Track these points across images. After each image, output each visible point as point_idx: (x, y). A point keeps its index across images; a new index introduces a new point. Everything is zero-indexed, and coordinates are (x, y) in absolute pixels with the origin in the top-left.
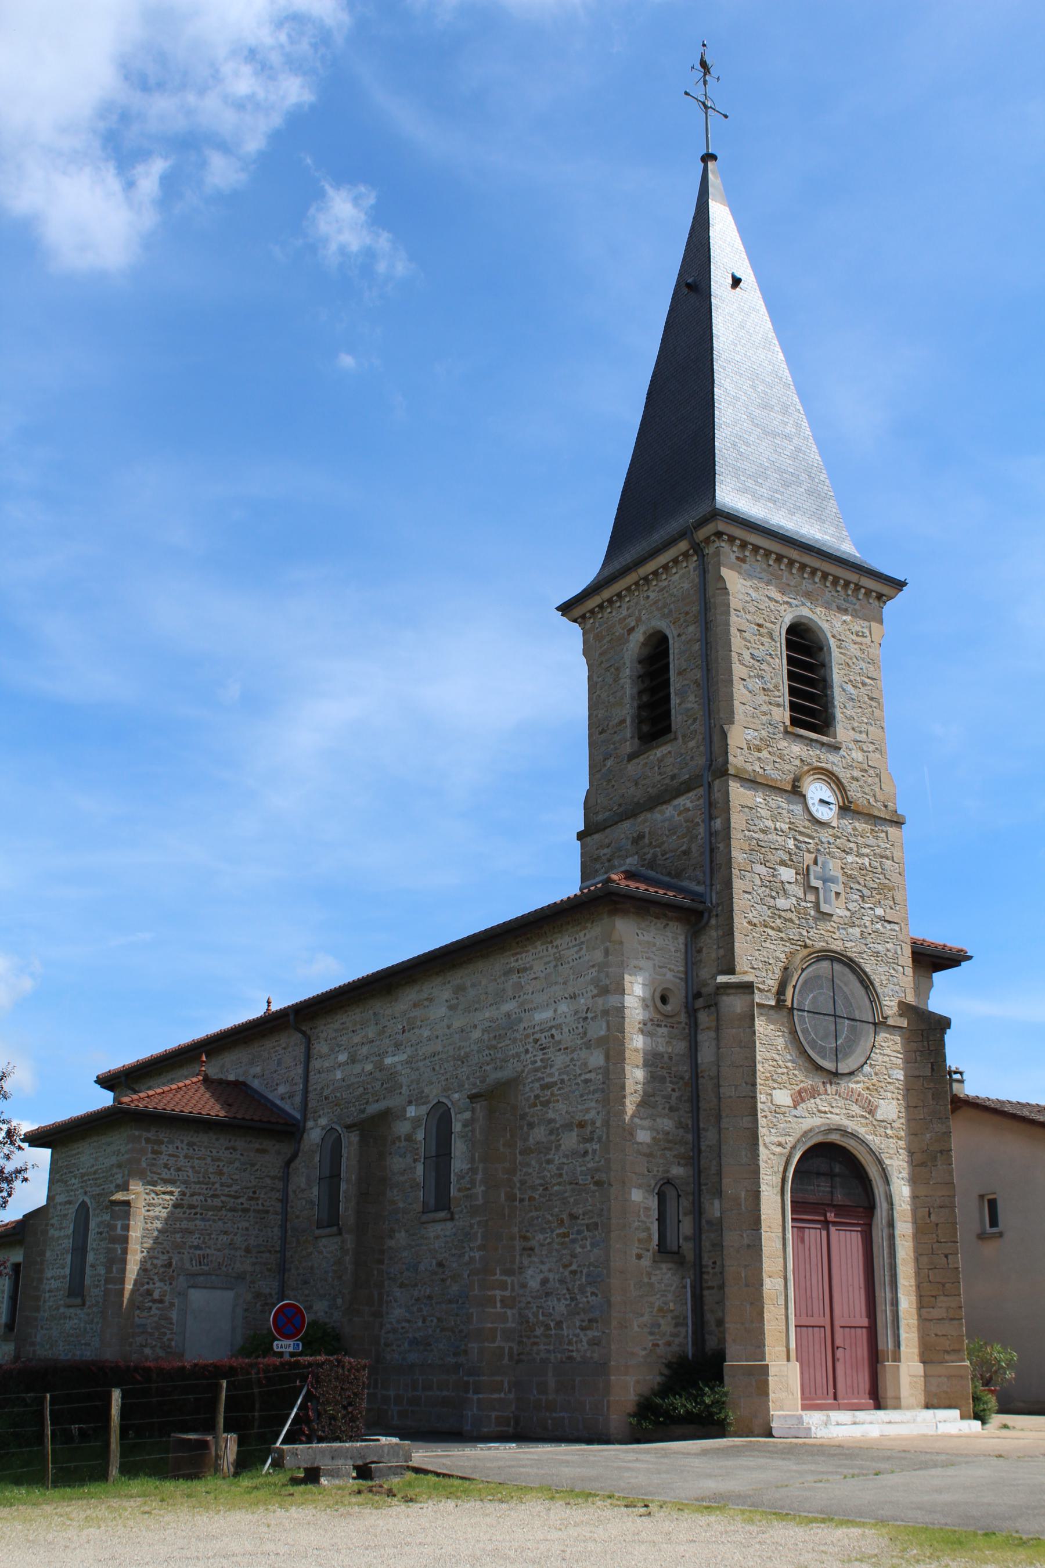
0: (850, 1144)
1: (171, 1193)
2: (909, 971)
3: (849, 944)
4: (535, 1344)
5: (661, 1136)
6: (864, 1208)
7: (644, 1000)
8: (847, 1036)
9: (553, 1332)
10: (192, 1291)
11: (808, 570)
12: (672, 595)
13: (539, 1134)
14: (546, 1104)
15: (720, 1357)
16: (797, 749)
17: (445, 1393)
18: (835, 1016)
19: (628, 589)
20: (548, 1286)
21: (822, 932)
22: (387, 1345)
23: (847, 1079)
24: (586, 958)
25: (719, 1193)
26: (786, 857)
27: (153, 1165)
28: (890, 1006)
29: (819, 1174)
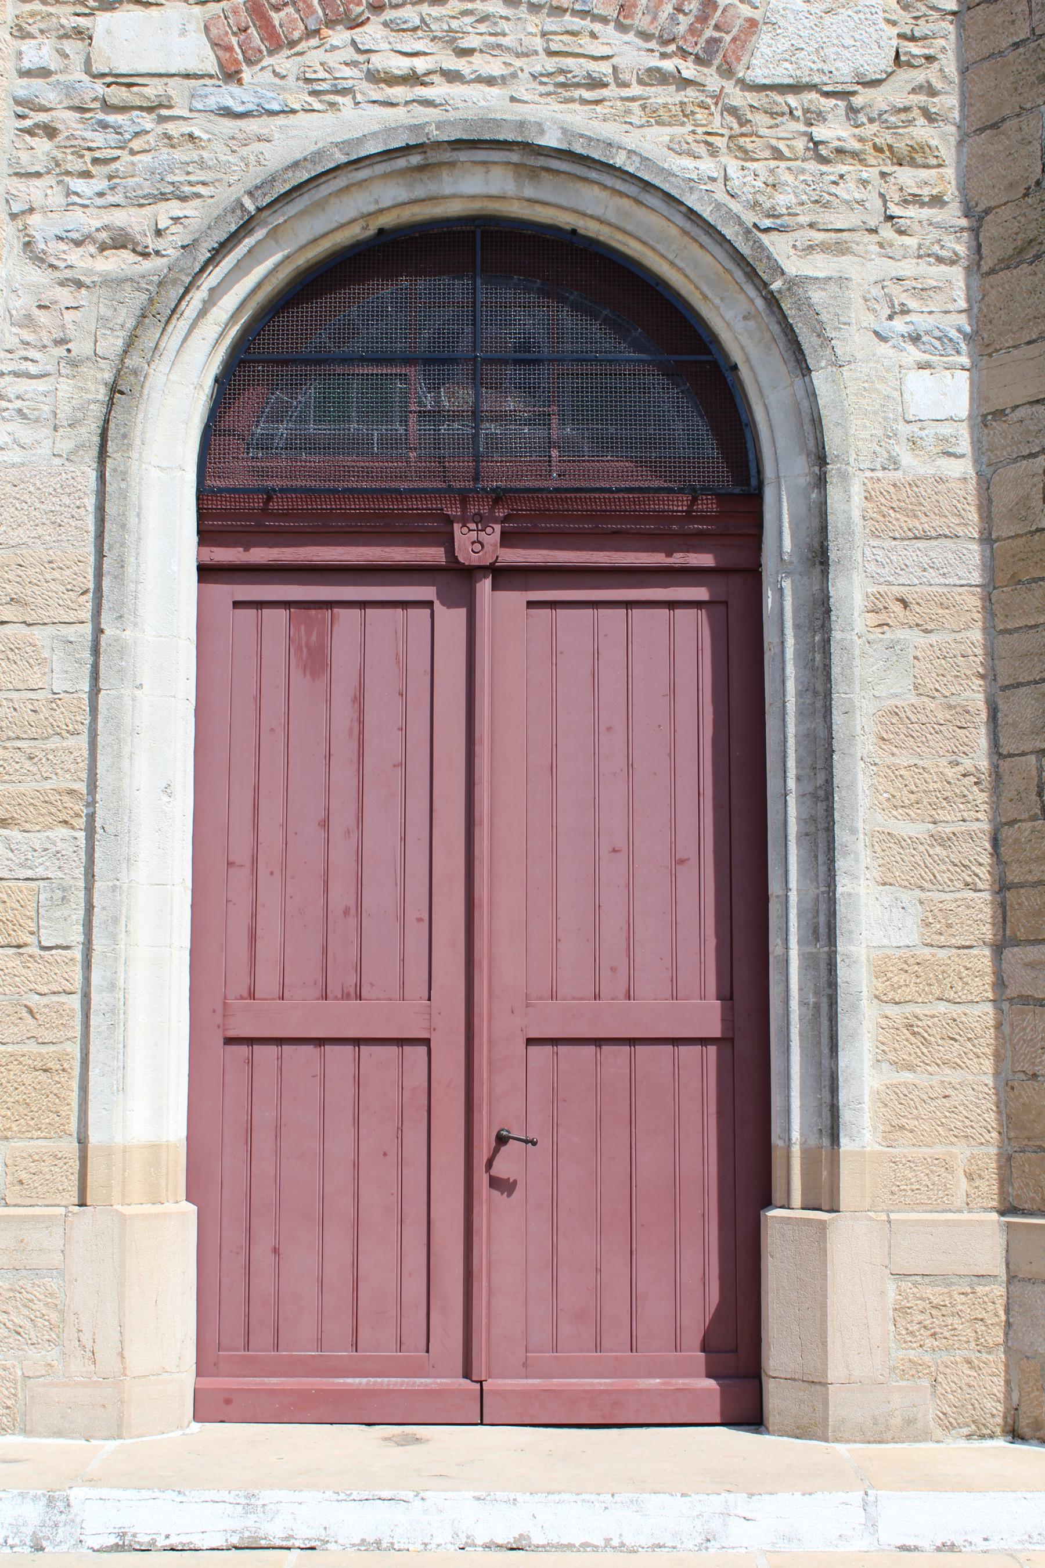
6: (721, 497)
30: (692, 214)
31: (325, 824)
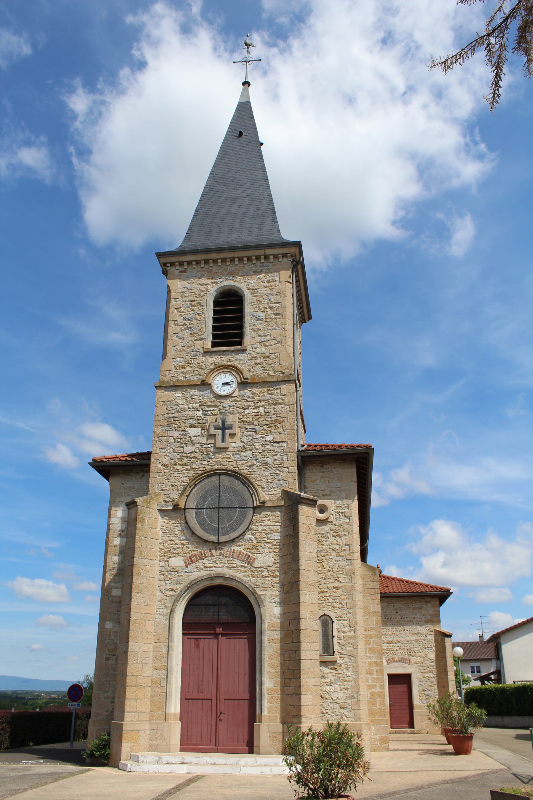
21: (220, 459)
26: (195, 422)
30: (246, 586)
31: (199, 669)
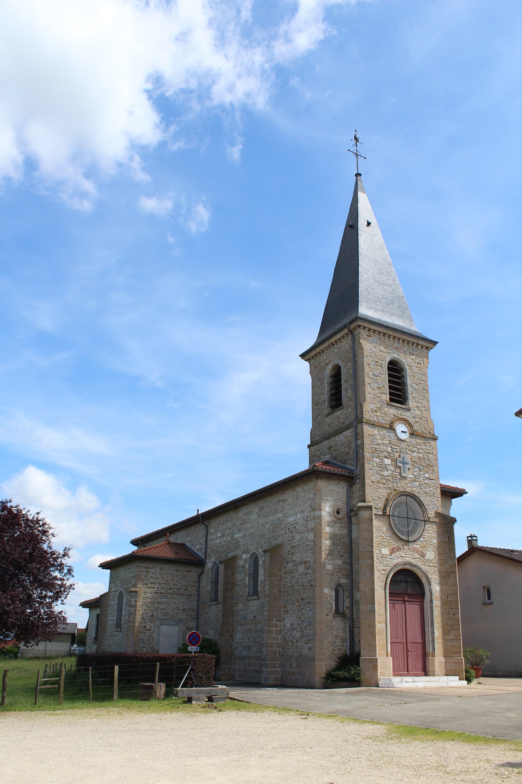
0: (414, 569)
1: (153, 588)
2: (439, 499)
3: (414, 489)
4: (288, 649)
5: (337, 567)
7: (329, 513)
8: (413, 526)
9: (295, 644)
10: (162, 626)
11: (397, 339)
12: (342, 350)
13: (290, 566)
14: (293, 554)
15: (359, 655)
16: (392, 411)
17: (256, 668)
18: (407, 518)
19: (326, 348)
20: (293, 626)
22: (235, 648)
23: (412, 543)
24: (307, 496)
25: (358, 589)
26: (387, 455)
27: (146, 577)
28: (431, 513)
29: (401, 582)
